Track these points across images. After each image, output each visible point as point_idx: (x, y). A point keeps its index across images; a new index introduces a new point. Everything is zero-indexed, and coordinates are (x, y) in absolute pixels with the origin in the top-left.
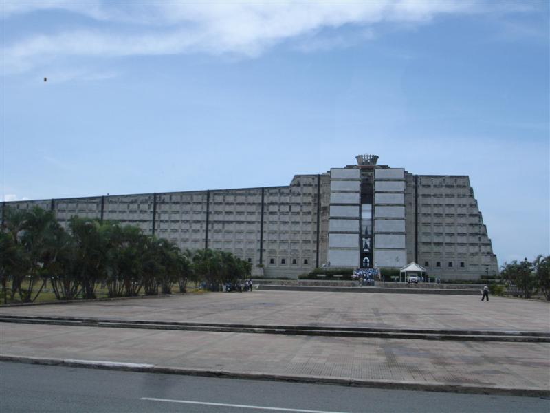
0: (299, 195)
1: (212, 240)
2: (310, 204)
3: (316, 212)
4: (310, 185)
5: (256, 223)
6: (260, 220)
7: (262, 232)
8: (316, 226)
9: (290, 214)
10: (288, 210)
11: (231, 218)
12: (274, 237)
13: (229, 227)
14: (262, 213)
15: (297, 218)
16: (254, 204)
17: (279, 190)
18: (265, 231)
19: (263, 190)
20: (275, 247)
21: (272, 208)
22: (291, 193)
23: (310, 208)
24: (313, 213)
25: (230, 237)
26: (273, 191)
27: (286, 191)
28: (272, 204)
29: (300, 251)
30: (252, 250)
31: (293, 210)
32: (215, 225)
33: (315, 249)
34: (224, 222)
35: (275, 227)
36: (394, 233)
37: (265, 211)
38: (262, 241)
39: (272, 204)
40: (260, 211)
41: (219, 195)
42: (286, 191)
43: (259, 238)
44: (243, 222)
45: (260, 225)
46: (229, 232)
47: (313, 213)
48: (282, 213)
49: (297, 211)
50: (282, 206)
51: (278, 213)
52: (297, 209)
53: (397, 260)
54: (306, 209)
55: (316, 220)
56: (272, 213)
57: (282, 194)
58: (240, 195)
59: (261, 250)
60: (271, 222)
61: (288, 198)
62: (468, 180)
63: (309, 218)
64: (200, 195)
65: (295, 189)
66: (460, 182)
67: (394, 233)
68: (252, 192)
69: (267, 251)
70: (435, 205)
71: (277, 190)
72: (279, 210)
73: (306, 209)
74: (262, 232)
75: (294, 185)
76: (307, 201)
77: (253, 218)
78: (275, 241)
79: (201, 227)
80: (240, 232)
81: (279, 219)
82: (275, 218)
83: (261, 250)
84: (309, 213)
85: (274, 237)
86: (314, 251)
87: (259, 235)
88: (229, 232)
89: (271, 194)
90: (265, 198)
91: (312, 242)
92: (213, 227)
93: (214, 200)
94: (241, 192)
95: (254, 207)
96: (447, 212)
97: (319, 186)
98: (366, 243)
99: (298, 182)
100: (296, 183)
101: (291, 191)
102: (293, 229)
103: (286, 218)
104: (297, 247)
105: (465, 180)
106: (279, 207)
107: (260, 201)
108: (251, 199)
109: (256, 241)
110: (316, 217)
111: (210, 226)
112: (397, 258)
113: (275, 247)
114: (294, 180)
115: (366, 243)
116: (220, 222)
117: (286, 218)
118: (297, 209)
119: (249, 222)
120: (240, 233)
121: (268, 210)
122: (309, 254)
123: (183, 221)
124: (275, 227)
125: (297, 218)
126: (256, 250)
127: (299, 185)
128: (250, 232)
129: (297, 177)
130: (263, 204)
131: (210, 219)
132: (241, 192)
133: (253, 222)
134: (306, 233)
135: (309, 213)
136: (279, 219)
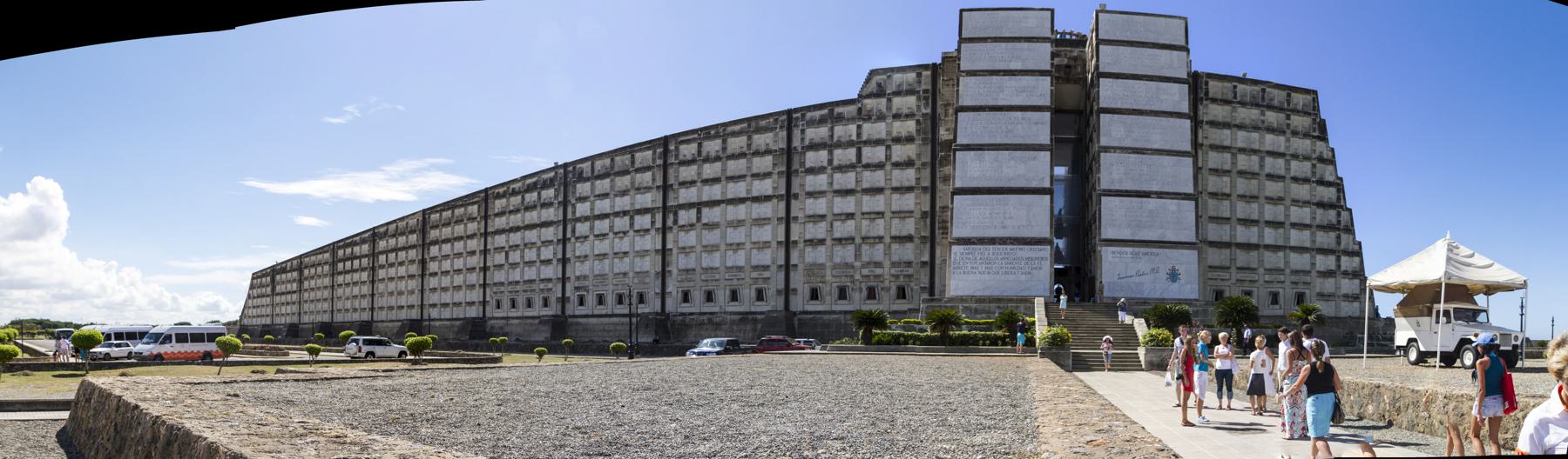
0: (881, 117)
2: (910, 139)
3: (928, 159)
4: (910, 92)
5: (775, 201)
6: (783, 192)
7: (788, 220)
8: (928, 197)
10: (854, 160)
11: (715, 192)
12: (819, 231)
14: (789, 175)
15: (877, 178)
16: (768, 152)
17: (830, 113)
18: (796, 218)
19: (789, 119)
20: (818, 255)
21: (814, 158)
22: (863, 116)
23: (909, 151)
24: (918, 163)
25: (712, 237)
26: (817, 114)
27: (850, 110)
28: (814, 146)
29: (887, 264)
30: (766, 268)
31: (864, 161)
32: (682, 213)
33: (926, 258)
35: (819, 206)
36: (1161, 195)
37: (795, 166)
38: (788, 244)
39: (814, 146)
40: (784, 169)
42: (850, 110)
43: (782, 238)
45: (782, 205)
46: (711, 226)
47: (918, 163)
50: (838, 152)
51: (829, 170)
52: (878, 154)
53: (1173, 276)
54: (900, 152)
55: (926, 183)
56: (812, 171)
57: (840, 119)
58: (734, 134)
59: (788, 267)
60: (810, 194)
61: (853, 128)
63: (908, 176)
65: (869, 103)
67: (1161, 195)
68: (763, 123)
69: (801, 267)
71: (825, 111)
72: (830, 161)
73: (900, 152)
74: (788, 220)
75: (869, 96)
76: (904, 134)
77: (765, 187)
78: (822, 242)
80: (739, 223)
82: (820, 181)
83: (788, 267)
84: (909, 163)
85: (819, 231)
86: (924, 263)
87: (782, 229)
88: (711, 226)
89: (812, 123)
90: (797, 133)
91: (916, 240)
95: (769, 159)
97: (933, 95)
99: (879, 85)
100: (873, 86)
101: (860, 110)
102: (865, 209)
103: (847, 180)
104: (878, 252)
106: (831, 153)
107: (783, 145)
108: (761, 140)
110: (927, 173)
113: (818, 255)
114: (867, 81)
117: (847, 180)
118: (878, 154)
119: (756, 199)
121: (803, 164)
122: (911, 271)
124: (819, 206)
125: (877, 178)
126: (774, 268)
127: (880, 93)
128: (760, 222)
129: (873, 73)
130: (789, 152)
133: (768, 198)
134: (902, 214)
135: (909, 163)
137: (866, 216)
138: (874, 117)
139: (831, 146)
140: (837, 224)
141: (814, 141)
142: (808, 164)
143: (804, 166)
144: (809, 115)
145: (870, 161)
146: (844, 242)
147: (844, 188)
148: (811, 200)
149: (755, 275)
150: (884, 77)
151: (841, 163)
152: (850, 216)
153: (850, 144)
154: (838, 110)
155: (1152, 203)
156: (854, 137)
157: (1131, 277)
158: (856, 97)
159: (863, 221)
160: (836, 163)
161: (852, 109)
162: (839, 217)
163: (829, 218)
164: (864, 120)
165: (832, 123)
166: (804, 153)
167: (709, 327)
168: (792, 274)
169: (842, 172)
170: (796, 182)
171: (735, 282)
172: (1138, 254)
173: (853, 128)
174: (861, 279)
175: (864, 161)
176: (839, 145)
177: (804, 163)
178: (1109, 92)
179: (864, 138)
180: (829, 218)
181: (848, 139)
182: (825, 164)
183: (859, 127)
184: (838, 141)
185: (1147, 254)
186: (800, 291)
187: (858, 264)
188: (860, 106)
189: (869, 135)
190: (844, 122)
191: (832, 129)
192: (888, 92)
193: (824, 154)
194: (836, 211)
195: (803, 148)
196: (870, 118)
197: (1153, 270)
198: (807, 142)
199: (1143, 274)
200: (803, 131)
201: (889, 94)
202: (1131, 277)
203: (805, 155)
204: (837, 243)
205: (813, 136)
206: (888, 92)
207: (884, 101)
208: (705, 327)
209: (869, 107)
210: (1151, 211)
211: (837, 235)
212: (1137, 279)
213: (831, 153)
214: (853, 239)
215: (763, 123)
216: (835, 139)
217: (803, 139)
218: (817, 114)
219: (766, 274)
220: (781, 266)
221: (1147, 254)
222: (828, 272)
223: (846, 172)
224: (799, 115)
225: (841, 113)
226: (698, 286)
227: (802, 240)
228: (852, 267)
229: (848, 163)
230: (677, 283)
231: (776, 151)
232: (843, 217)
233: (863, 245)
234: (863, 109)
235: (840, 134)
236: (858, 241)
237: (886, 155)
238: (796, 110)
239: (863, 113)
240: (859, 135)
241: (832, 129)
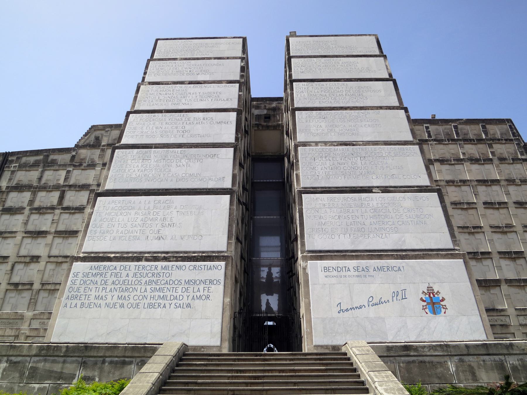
9: (57, 212)
26: (32, 159)
31: (66, 204)
39: (19, 188)
48: (40, 210)
49: (77, 204)
50: (41, 195)
51: (27, 212)
62: (512, 127)
65: (84, 153)
66: (496, 130)
70: (448, 182)
71: (41, 157)
72: (31, 202)
75: (84, 147)
81: (26, 223)
89: (23, 167)
96: (483, 198)
98: (268, 303)
100: (92, 139)
101: (73, 157)
105: (506, 127)
112: (430, 292)
115: (268, 303)
129: (94, 128)
136: (26, 223)
137: (52, 259)
138: (85, 165)
139: (36, 187)
140: (18, 267)
141: (21, 183)
142: (9, 204)
143: (4, 206)
144: (24, 160)
145: (70, 204)
146: (20, 287)
147: (38, 230)
150: (103, 132)
151: (42, 204)
152: (35, 259)
153: (57, 187)
154: (52, 157)
155: (376, 198)
156: (61, 182)
157: (361, 307)
158: (73, 146)
159: (49, 264)
160: (36, 204)
161: (67, 157)
162: (23, 260)
163: (11, 261)
164: (75, 166)
165: (44, 166)
166: (8, 193)
169: (41, 214)
172: (366, 269)
173: (63, 173)
174: (28, 334)
175: (66, 204)
176: (45, 188)
177: (4, 201)
178: (306, 94)
179: (72, 182)
180: (11, 261)
181: (55, 183)
182: (25, 205)
183: (68, 172)
184: (45, 184)
185: (381, 269)
188: (74, 153)
189: (77, 180)
190: (56, 167)
191: (43, 172)
192: (103, 144)
193: (27, 196)
194: (23, 252)
195: (7, 187)
196: (81, 165)
197: (396, 294)
198: (14, 183)
199: (381, 302)
200: (13, 172)
201: (104, 146)
202: (361, 307)
203: (7, 195)
204: (12, 287)
205: (22, 178)
206: (103, 144)
207: (98, 152)
209: (82, 157)
210: (375, 210)
211: (16, 279)
212: (371, 312)
213: (34, 194)
214: (32, 284)
216: (43, 181)
217: (10, 180)
218: (32, 159)
221: (381, 269)
223: (44, 214)
224: (14, 158)
225: (56, 160)
228: (22, 318)
229: (49, 205)
233: (42, 293)
234: (76, 156)
235: (50, 178)
236: (37, 286)
237: (88, 199)
238: (13, 154)
239: (76, 159)
240: (66, 179)
241: (43, 172)
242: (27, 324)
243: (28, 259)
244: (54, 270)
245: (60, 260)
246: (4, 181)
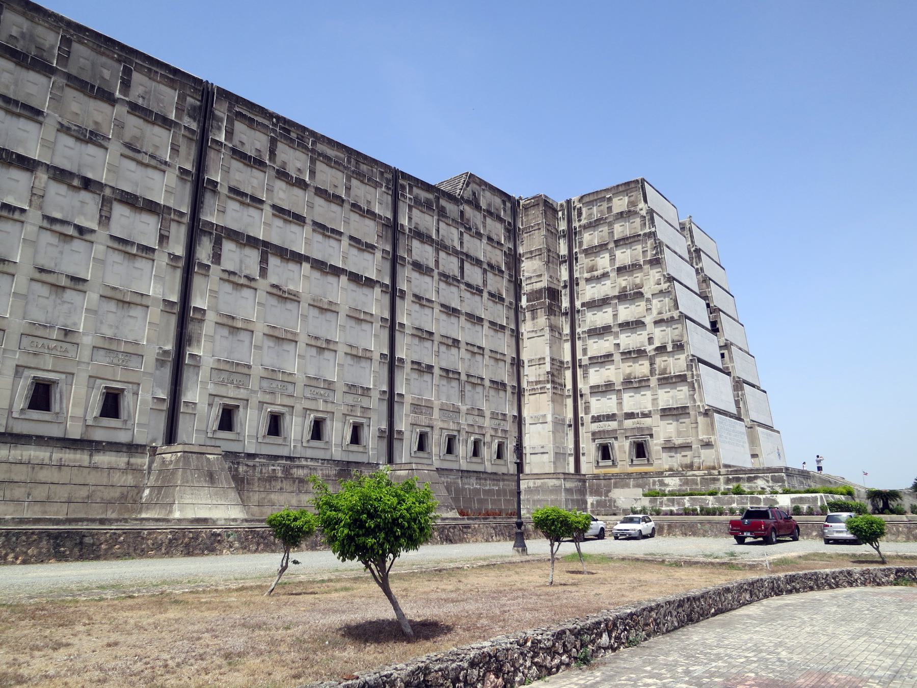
1: (211, 317)
5: (378, 290)
13: (279, 272)
34: (266, 249)
41: (251, 122)
44: (336, 271)
46: (282, 295)
58: (328, 160)
59: (391, 398)
64: (171, 84)
71: (430, 196)
79: (163, 238)
83: (391, 398)
88: (282, 295)
89: (417, 202)
92: (217, 257)
93: (230, 134)
94: (331, 153)
108: (362, 192)
109: (376, 356)
111: (204, 253)
116: (252, 242)
120: (322, 310)
123: (60, 175)
126: (375, 395)
131: (210, 216)
132: (331, 153)
146: (451, 375)
148: (417, 307)
149: (350, 399)
167: (287, 485)
168: (396, 407)
170: (406, 274)
171: (321, 406)
174: (467, 430)
186: (407, 435)
187: (463, 408)
208: (279, 485)
215: (364, 168)
219: (365, 402)
220: (384, 392)
222: (436, 414)
226: (254, 401)
227: (409, 361)
230: (211, 388)
231: (380, 217)
232: (450, 342)
242: (464, 418)
243: (450, 342)
244: (470, 360)
245: (476, 350)
246: (402, 219)
